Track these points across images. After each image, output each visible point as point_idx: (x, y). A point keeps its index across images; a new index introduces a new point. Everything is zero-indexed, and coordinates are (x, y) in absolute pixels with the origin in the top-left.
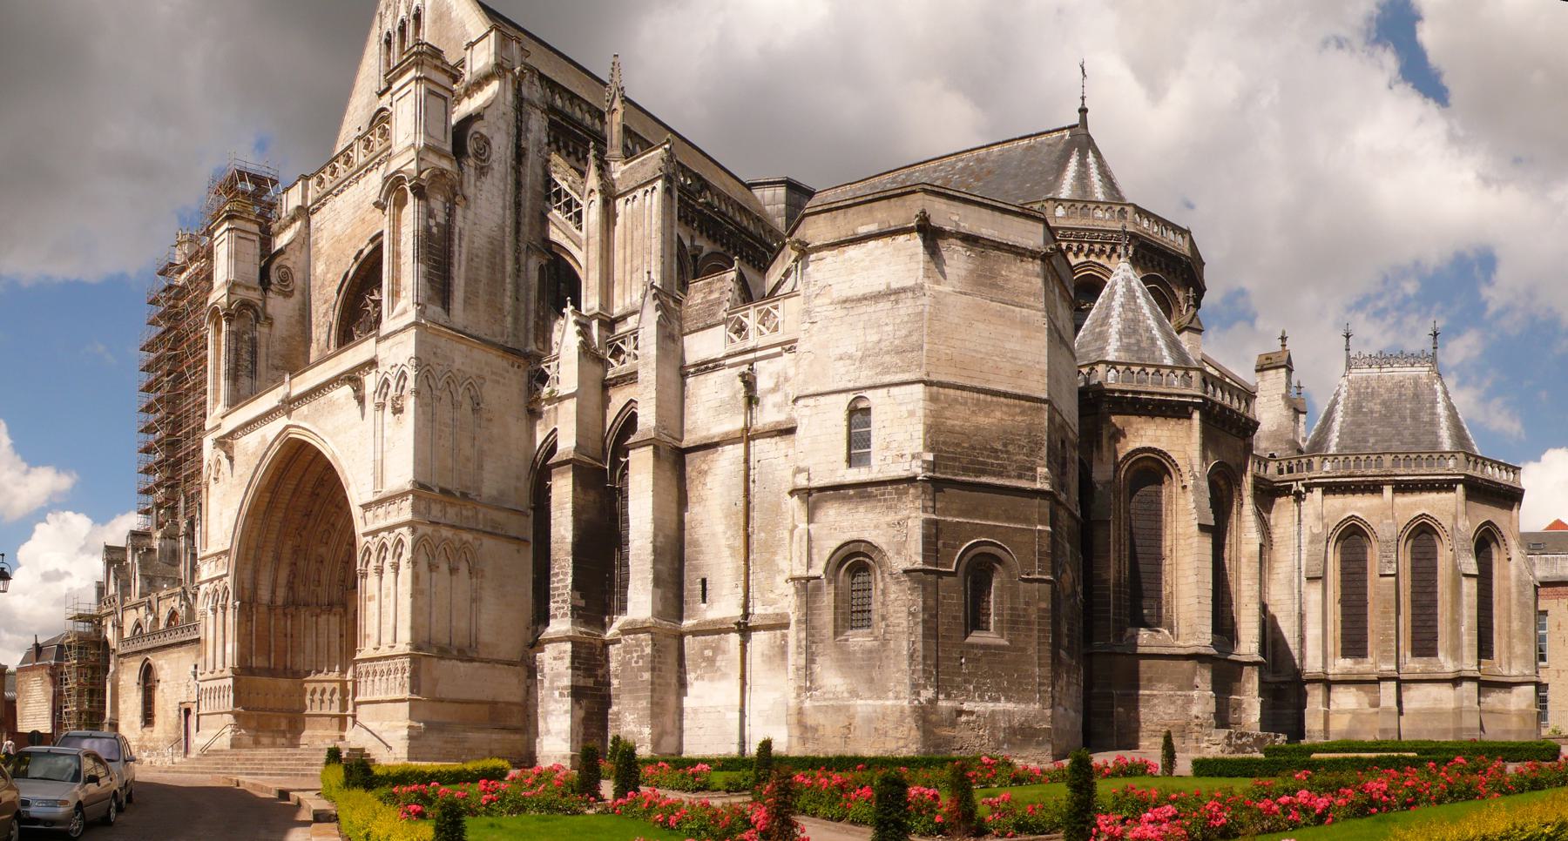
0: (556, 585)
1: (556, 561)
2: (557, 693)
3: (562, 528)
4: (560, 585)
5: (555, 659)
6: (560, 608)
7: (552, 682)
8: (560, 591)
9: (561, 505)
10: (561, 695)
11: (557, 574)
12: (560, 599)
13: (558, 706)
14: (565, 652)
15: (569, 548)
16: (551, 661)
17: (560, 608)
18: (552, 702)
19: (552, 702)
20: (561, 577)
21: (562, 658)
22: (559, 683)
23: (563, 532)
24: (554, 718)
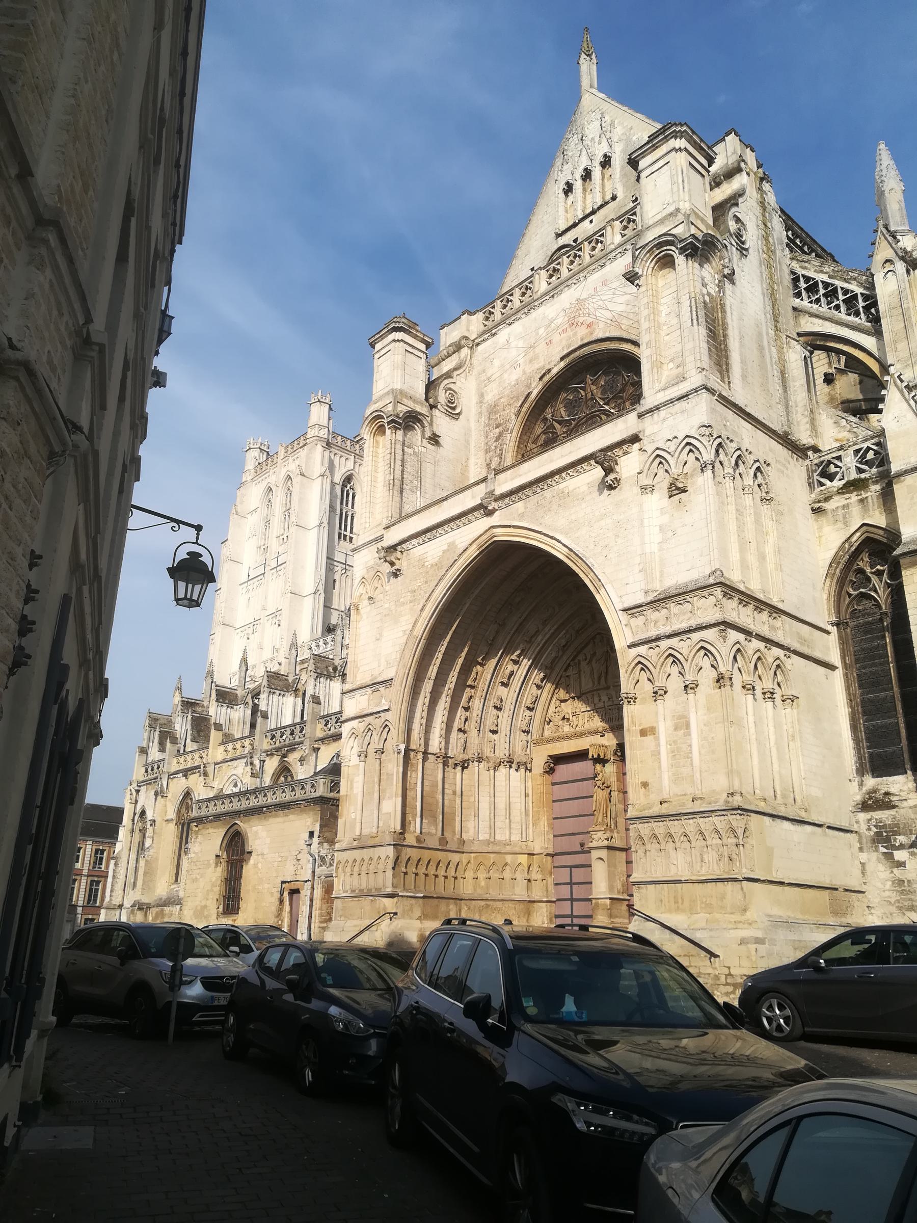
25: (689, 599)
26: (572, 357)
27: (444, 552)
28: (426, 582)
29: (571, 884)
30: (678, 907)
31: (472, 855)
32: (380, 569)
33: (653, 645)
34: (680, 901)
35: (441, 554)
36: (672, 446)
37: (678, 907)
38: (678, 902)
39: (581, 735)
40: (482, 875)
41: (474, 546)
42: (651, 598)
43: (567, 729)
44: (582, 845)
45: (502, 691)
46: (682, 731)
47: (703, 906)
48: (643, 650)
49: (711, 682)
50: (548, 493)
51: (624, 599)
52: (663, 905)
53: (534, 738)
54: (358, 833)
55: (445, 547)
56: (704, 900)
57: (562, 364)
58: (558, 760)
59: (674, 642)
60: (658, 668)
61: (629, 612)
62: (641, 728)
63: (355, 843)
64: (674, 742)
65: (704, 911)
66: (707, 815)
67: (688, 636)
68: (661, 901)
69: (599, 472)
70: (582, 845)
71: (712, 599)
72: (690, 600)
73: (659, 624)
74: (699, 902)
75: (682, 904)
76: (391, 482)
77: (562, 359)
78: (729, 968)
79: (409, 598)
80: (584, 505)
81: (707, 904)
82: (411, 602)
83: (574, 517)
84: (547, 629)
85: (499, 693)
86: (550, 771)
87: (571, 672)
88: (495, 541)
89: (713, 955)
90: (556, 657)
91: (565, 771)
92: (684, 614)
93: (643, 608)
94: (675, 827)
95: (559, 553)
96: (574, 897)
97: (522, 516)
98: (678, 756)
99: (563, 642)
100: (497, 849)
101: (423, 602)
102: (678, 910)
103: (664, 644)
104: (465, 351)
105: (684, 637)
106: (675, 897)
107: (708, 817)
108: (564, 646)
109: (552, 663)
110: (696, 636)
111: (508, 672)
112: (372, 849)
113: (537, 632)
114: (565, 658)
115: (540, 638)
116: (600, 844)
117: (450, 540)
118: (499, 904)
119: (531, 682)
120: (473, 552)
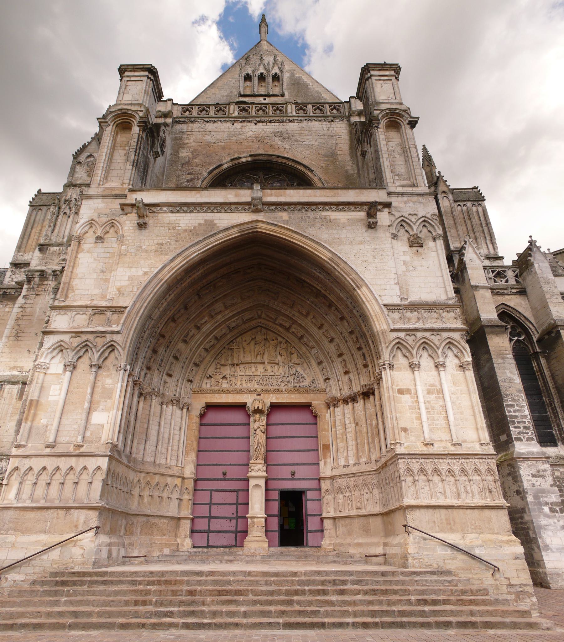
0: (512, 414)
1: (508, 395)
2: (546, 509)
3: (507, 371)
4: (517, 414)
5: (534, 476)
6: (523, 433)
7: (536, 497)
8: (519, 419)
9: (501, 355)
10: (552, 510)
11: (512, 406)
12: (521, 425)
13: (551, 521)
14: (544, 471)
15: (521, 387)
16: (530, 478)
17: (523, 433)
18: (542, 517)
19: (542, 517)
20: (516, 408)
21: (543, 476)
22: (546, 499)
23: (509, 375)
24: (550, 533)
25: (436, 310)
26: (257, 158)
27: (200, 224)
28: (176, 241)
29: (210, 504)
30: (451, 528)
31: (143, 475)
32: (117, 218)
33: (410, 333)
34: (452, 522)
35: (196, 225)
36: (413, 219)
37: (451, 528)
38: (450, 524)
39: (241, 391)
40: (146, 493)
41: (236, 229)
42: (406, 303)
43: (225, 385)
44: (225, 474)
45: (181, 345)
46: (434, 395)
47: (473, 527)
48: (402, 335)
49: (454, 366)
50: (312, 215)
51: (383, 298)
52: (436, 525)
53: (194, 387)
54: (51, 440)
55: (202, 222)
56: (473, 522)
57: (249, 159)
58: (210, 407)
59: (427, 334)
60: (416, 349)
61: (388, 308)
62: (398, 388)
63: (48, 451)
64: (428, 401)
65: (474, 531)
66: (469, 457)
67: (439, 333)
68: (434, 522)
69: (362, 215)
70: (293, 474)
71: (452, 314)
72: (437, 311)
73: (412, 321)
74: (469, 525)
75: (454, 525)
76: (136, 161)
77: (251, 156)
78: (508, 579)
79: (153, 248)
80: (345, 231)
81: (477, 526)
82: (156, 251)
83: (337, 236)
84: (226, 312)
85: (179, 347)
86: (202, 416)
87: (234, 346)
88: (257, 232)
89: (496, 569)
90: (225, 334)
91: (212, 417)
92: (432, 318)
93: (401, 308)
94: (443, 465)
95: (324, 255)
96: (212, 515)
97: (286, 222)
98: (432, 413)
99: (234, 325)
100: (162, 470)
101: (175, 254)
102: (451, 530)
103: (419, 335)
104: (169, 120)
105: (435, 333)
106: (446, 519)
107: (469, 459)
108: (233, 328)
109: (221, 337)
110: (445, 335)
111: (191, 334)
112: (74, 459)
113: (221, 311)
114: (229, 336)
115: (219, 317)
116: (259, 474)
117: (207, 218)
118: (156, 520)
119: (202, 346)
120: (234, 233)
